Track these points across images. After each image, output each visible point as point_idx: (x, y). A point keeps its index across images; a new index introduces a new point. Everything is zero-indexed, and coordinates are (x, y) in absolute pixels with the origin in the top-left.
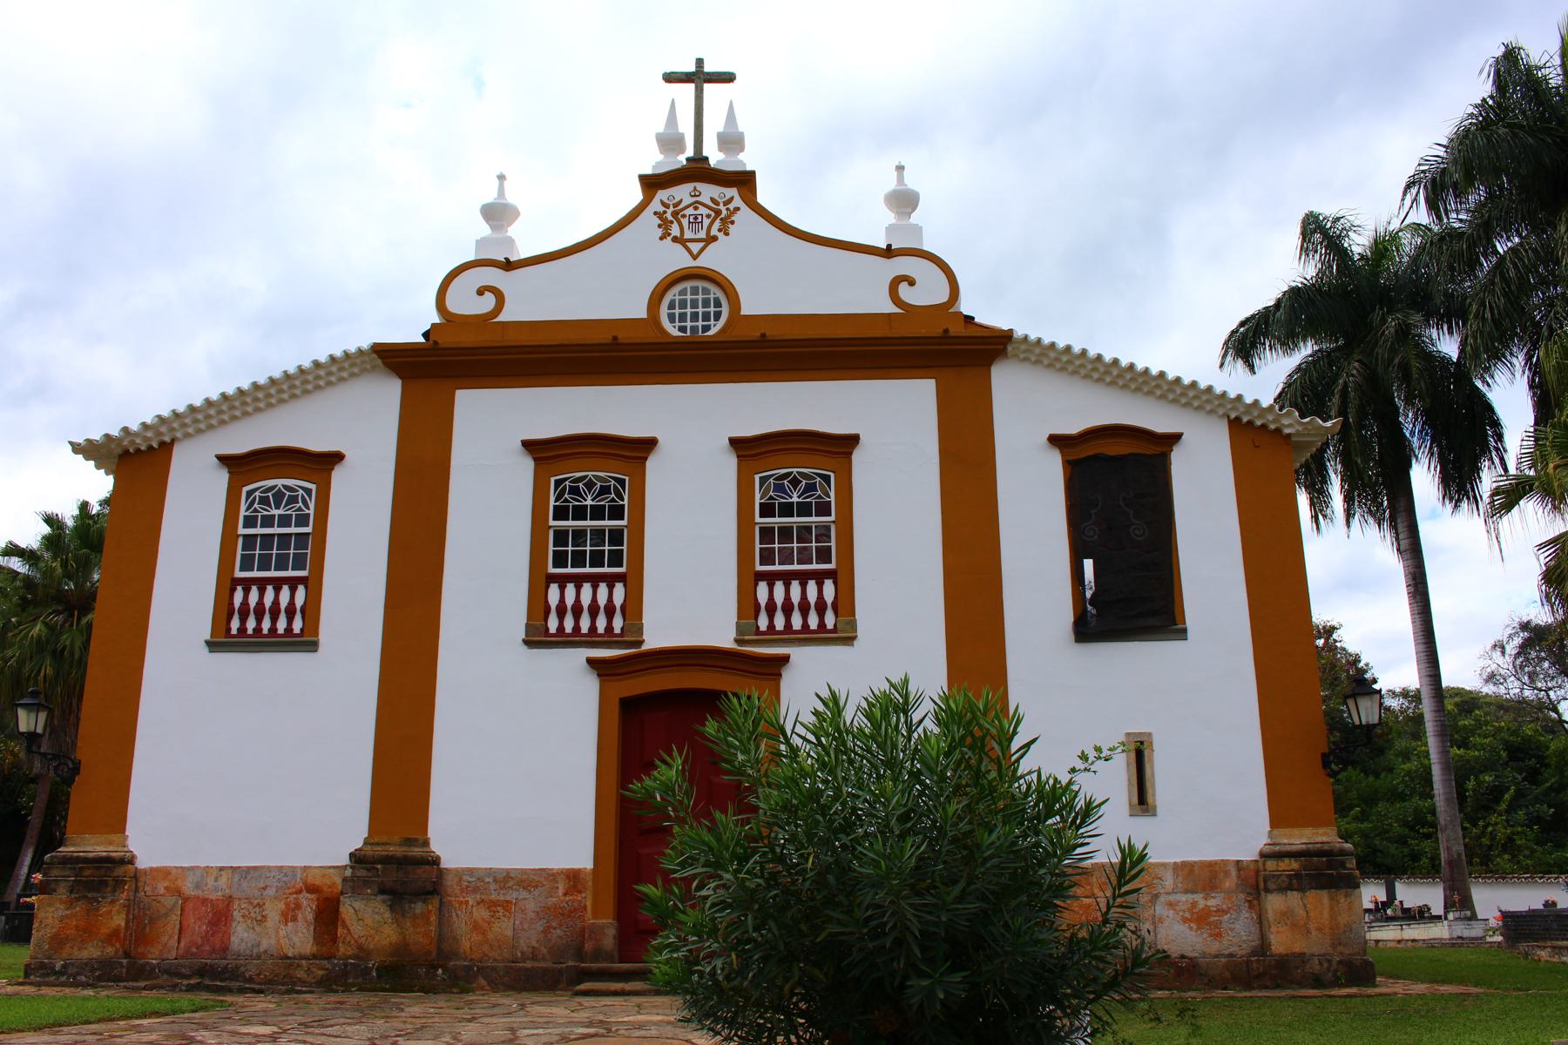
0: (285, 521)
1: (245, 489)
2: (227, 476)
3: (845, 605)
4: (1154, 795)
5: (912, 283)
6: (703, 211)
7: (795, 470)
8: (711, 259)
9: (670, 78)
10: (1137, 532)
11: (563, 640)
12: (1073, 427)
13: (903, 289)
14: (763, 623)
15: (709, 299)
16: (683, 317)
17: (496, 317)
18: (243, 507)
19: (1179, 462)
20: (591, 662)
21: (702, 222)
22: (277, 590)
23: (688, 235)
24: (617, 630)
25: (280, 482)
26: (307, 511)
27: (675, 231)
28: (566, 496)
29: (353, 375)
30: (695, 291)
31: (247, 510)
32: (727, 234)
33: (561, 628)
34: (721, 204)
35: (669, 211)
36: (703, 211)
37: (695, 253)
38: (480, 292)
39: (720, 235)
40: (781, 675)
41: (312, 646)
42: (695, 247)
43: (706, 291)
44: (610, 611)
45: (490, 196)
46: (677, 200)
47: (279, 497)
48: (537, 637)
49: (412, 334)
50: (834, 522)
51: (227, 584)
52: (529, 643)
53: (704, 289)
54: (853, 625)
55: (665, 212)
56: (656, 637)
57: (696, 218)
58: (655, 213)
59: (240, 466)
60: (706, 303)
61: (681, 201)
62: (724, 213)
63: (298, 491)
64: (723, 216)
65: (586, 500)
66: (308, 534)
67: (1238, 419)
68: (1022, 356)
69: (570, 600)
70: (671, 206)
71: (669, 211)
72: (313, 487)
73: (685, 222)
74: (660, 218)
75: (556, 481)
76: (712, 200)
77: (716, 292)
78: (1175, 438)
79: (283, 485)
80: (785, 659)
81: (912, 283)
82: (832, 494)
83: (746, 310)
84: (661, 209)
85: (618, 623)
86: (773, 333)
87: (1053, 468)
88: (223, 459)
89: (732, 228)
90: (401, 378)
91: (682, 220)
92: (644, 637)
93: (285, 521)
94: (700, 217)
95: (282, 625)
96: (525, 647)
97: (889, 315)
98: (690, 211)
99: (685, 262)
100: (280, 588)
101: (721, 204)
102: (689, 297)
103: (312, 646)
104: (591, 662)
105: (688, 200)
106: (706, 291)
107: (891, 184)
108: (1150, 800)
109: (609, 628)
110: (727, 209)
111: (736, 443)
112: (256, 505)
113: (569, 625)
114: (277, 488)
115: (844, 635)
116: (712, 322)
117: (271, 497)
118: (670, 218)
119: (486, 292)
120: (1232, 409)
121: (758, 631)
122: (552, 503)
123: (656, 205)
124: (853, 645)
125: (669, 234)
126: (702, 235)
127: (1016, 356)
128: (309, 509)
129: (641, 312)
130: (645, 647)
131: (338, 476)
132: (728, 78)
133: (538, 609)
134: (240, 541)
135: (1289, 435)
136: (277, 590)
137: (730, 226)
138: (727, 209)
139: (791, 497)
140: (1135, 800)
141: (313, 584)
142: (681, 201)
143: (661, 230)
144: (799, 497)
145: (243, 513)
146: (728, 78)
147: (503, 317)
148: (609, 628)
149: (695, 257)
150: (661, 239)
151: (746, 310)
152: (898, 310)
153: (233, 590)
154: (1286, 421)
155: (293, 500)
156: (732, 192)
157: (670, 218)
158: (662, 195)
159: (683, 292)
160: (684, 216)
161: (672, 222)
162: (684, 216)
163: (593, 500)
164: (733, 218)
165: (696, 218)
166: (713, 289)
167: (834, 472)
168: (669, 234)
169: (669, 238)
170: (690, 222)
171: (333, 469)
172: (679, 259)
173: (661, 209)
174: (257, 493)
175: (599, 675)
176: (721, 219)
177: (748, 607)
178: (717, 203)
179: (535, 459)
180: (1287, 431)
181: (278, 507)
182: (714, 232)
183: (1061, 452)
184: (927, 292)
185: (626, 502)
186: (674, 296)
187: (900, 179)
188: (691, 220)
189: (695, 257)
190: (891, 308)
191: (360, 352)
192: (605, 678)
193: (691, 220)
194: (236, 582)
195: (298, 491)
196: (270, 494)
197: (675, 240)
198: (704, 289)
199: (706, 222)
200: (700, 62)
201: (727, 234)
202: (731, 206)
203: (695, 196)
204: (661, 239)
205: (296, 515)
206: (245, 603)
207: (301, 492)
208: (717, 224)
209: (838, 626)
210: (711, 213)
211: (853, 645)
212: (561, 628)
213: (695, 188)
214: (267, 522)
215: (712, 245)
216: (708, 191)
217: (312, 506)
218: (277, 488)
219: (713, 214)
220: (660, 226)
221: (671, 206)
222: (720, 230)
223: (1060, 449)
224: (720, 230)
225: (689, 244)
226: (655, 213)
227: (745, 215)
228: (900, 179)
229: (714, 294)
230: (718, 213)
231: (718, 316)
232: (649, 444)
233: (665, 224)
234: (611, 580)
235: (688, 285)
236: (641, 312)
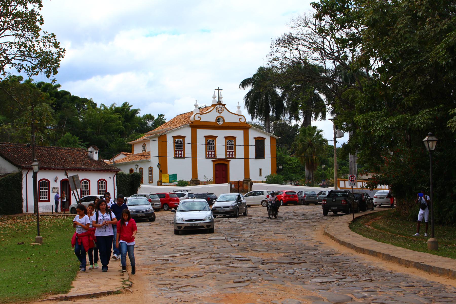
3: (235, 155)
8: (222, 115)
9: (215, 89)
12: (256, 137)
14: (227, 156)
16: (219, 122)
19: (265, 140)
20: (212, 160)
25: (179, 139)
27: (218, 111)
36: (221, 109)
42: (220, 113)
44: (213, 155)
45: (195, 104)
47: (179, 141)
51: (175, 151)
59: (174, 137)
69: (209, 153)
77: (222, 119)
83: (225, 121)
85: (214, 156)
87: (254, 141)
88: (173, 137)
89: (224, 111)
105: (219, 107)
107: (237, 105)
109: (213, 157)
123: (216, 108)
132: (222, 90)
133: (206, 154)
141: (184, 151)
146: (222, 90)
148: (213, 157)
151: (225, 121)
156: (223, 106)
158: (216, 106)
172: (218, 115)
177: (226, 155)
184: (243, 120)
187: (239, 105)
194: (176, 151)
200: (219, 88)
216: (221, 106)
228: (239, 105)
233: (217, 110)
235: (219, 118)
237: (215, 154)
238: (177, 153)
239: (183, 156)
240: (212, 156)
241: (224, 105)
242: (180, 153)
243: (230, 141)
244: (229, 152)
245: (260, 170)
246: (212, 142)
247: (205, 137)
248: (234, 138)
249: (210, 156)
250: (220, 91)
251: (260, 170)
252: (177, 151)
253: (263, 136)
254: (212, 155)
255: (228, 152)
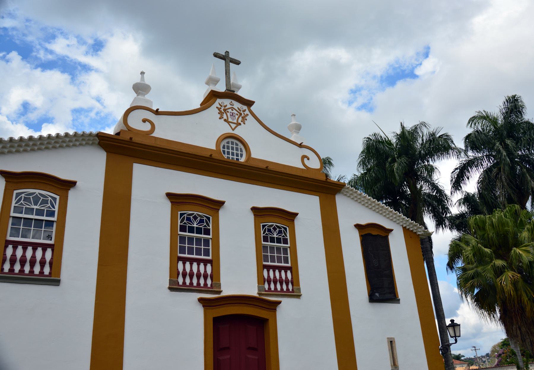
0: (40, 212)
1: (15, 192)
2: (5, 182)
3: (295, 281)
4: (397, 362)
5: (308, 159)
6: (234, 111)
7: (275, 224)
8: (239, 132)
10: (375, 263)
11: (190, 289)
12: (363, 222)
13: (305, 160)
15: (238, 148)
17: (151, 134)
18: (14, 202)
20: (201, 300)
21: (235, 116)
22: (35, 250)
23: (230, 120)
24: (209, 286)
25: (37, 191)
26: (53, 209)
27: (225, 117)
28: (185, 221)
29: (81, 145)
30: (232, 143)
31: (16, 203)
32: (245, 124)
33: (184, 283)
34: (242, 111)
35: (223, 108)
36: (234, 111)
37: (233, 128)
38: (144, 121)
39: (242, 123)
40: (276, 309)
41: (57, 282)
43: (237, 145)
44: (206, 277)
46: (225, 104)
48: (174, 287)
49: (110, 131)
50: (289, 247)
52: (171, 289)
53: (236, 143)
54: (299, 290)
55: (221, 108)
56: (227, 291)
57: (233, 114)
58: (217, 108)
60: (237, 149)
61: (226, 106)
62: (243, 115)
63: (48, 198)
64: (242, 116)
65: (194, 224)
66: (53, 221)
67: (405, 227)
68: (345, 193)
69: (188, 270)
70: (223, 107)
71: (223, 108)
72: (58, 197)
73: (229, 114)
74: (219, 110)
75: (180, 214)
76: (238, 108)
77: (240, 146)
78: (391, 230)
79: (38, 193)
80: (279, 303)
81: (308, 159)
82: (288, 235)
84: (219, 107)
85: (209, 282)
86: (271, 167)
89: (246, 122)
90: (106, 152)
91: (227, 113)
92: (222, 289)
93: (40, 212)
94: (234, 114)
95: (37, 269)
96: (169, 290)
97: (302, 169)
98: (230, 110)
99: (231, 131)
100: (36, 249)
101: (242, 111)
102: (230, 145)
103: (57, 282)
104: (201, 300)
105: (229, 106)
106: (237, 145)
108: (397, 364)
109: (206, 284)
110: (244, 114)
111: (254, 210)
112: (22, 201)
113: (188, 281)
114: (36, 194)
115: (295, 294)
116: (239, 158)
117: (41, 199)
118: (223, 111)
119: (146, 121)
120: (405, 224)
121: (266, 291)
122: (179, 224)
124: (300, 298)
125: (223, 118)
126: (235, 121)
127: (342, 193)
128: (54, 208)
129: (214, 147)
130: (224, 294)
131: (72, 193)
132: (237, 63)
133: (174, 273)
134: (11, 220)
135: (419, 235)
136: (35, 250)
137: (245, 120)
138: (244, 114)
139: (274, 235)
140: (393, 364)
142: (226, 106)
143: (219, 115)
144: (277, 235)
145: (13, 204)
146: (237, 63)
147: (153, 135)
148: (206, 284)
149: (233, 130)
150: (220, 118)
151: (253, 156)
152: (302, 167)
153: (6, 247)
154: (420, 230)
155: (45, 202)
156: (245, 107)
157: (223, 111)
158: (219, 101)
159: (228, 143)
160: (228, 112)
161: (223, 113)
162: (228, 112)
163: (197, 225)
164: (246, 118)
165: (233, 114)
166: (240, 144)
167: (288, 227)
168: (223, 118)
169: (223, 120)
170: (230, 115)
171: (69, 190)
172: (227, 129)
173: (219, 107)
174: (23, 195)
175: (203, 306)
176: (242, 117)
177: (261, 280)
178: (240, 110)
179: (171, 202)
180: (419, 233)
181: (36, 204)
182: (240, 121)
183: (358, 231)
184: (314, 164)
185: (211, 227)
186: (225, 143)
188: (231, 114)
189: (233, 130)
190: (302, 167)
191: (91, 134)
192: (206, 307)
193: (231, 114)
195: (48, 198)
196: (31, 197)
197: (225, 120)
198: (236, 143)
199: (237, 117)
201: (245, 124)
202: (246, 113)
203: (232, 105)
204: (220, 118)
205: (47, 210)
206: (14, 255)
207: (50, 198)
208: (240, 119)
209: (295, 290)
210: (238, 113)
211: (300, 298)
212: (184, 283)
213: (231, 102)
214: (30, 211)
215: (239, 127)
217: (57, 207)
218: (36, 194)
219: (239, 114)
220: (219, 113)
221: (223, 107)
222: (242, 121)
223: (358, 229)
224: (242, 121)
225: (230, 124)
226: (217, 108)
227: (250, 118)
229: (240, 146)
230: (241, 114)
231: (241, 156)
232: (221, 203)
233: (221, 113)
234: (206, 262)
235: (230, 140)
236: (214, 147)
237: (215, 276)
238: (14, 255)
239: (47, 270)
240: (202, 282)
241: (249, 103)
242: (34, 257)
243: (275, 229)
244: (274, 268)
245: (391, 343)
246: (201, 221)
247: (170, 196)
248: (291, 216)
249: (191, 283)
250: (232, 65)
251: (391, 343)
252: (15, 245)
253: (386, 224)
254: (199, 276)
255: (268, 268)
